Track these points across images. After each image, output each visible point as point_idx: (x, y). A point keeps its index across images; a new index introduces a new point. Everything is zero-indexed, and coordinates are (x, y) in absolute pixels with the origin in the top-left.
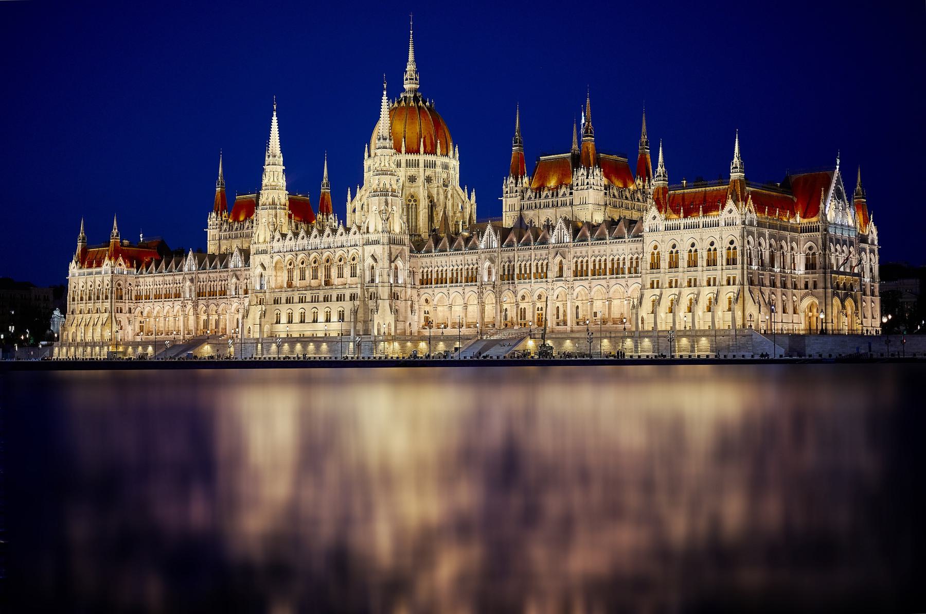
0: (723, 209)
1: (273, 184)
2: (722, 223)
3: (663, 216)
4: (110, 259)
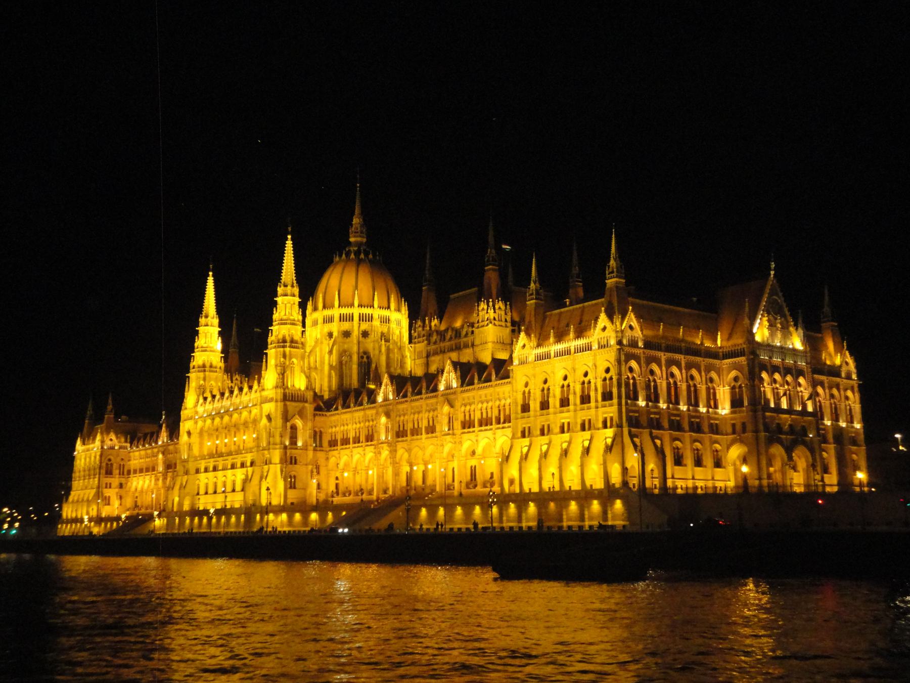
0: (595, 327)
1: (205, 345)
2: (595, 346)
3: (534, 342)
4: (102, 434)
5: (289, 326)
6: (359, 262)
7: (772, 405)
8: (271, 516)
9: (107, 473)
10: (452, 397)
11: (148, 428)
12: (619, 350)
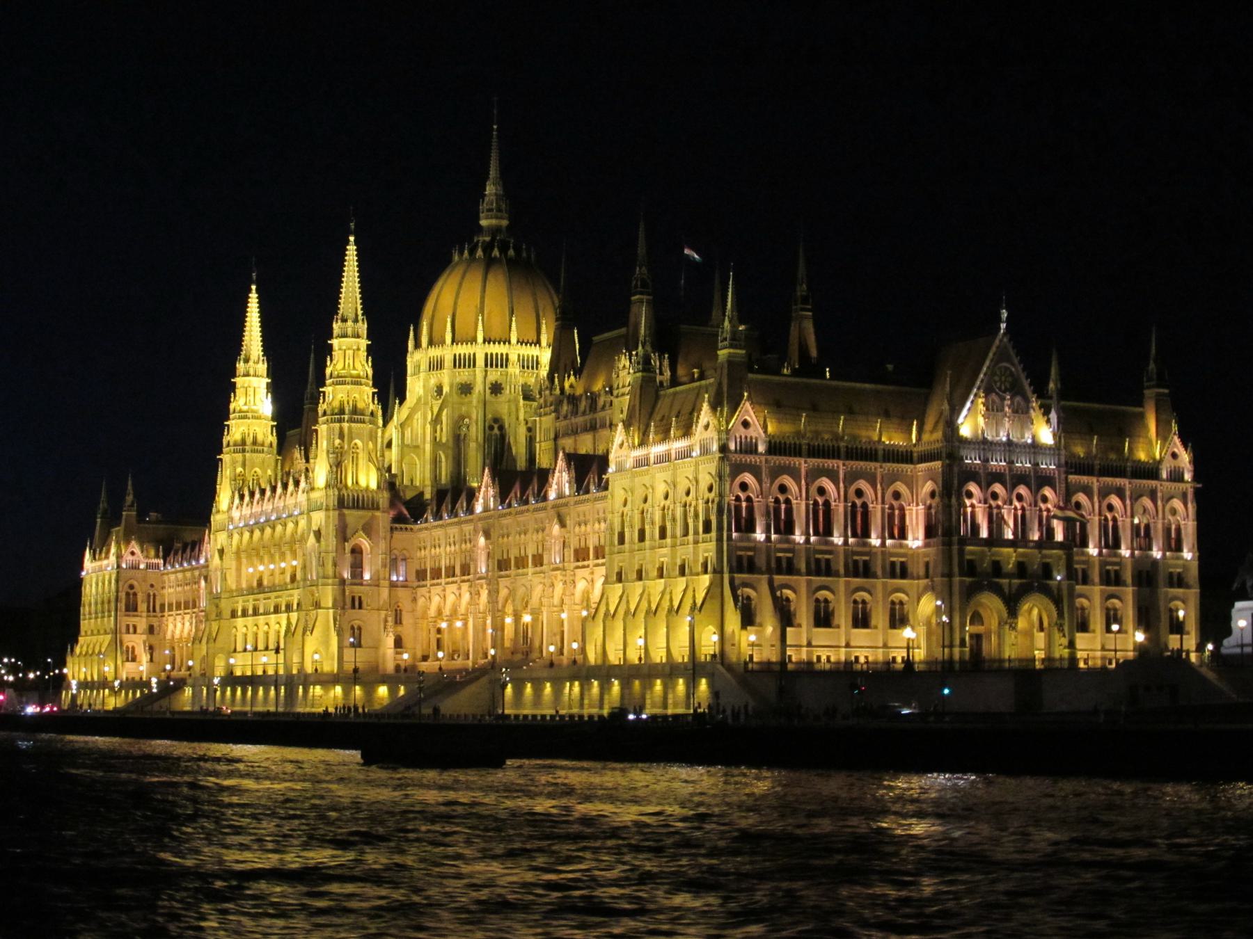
1: (245, 408)
4: (118, 543)
5: (349, 387)
6: (489, 263)
7: (984, 534)
8: (318, 690)
9: (127, 609)
10: (563, 510)
11: (189, 537)
12: (722, 459)
